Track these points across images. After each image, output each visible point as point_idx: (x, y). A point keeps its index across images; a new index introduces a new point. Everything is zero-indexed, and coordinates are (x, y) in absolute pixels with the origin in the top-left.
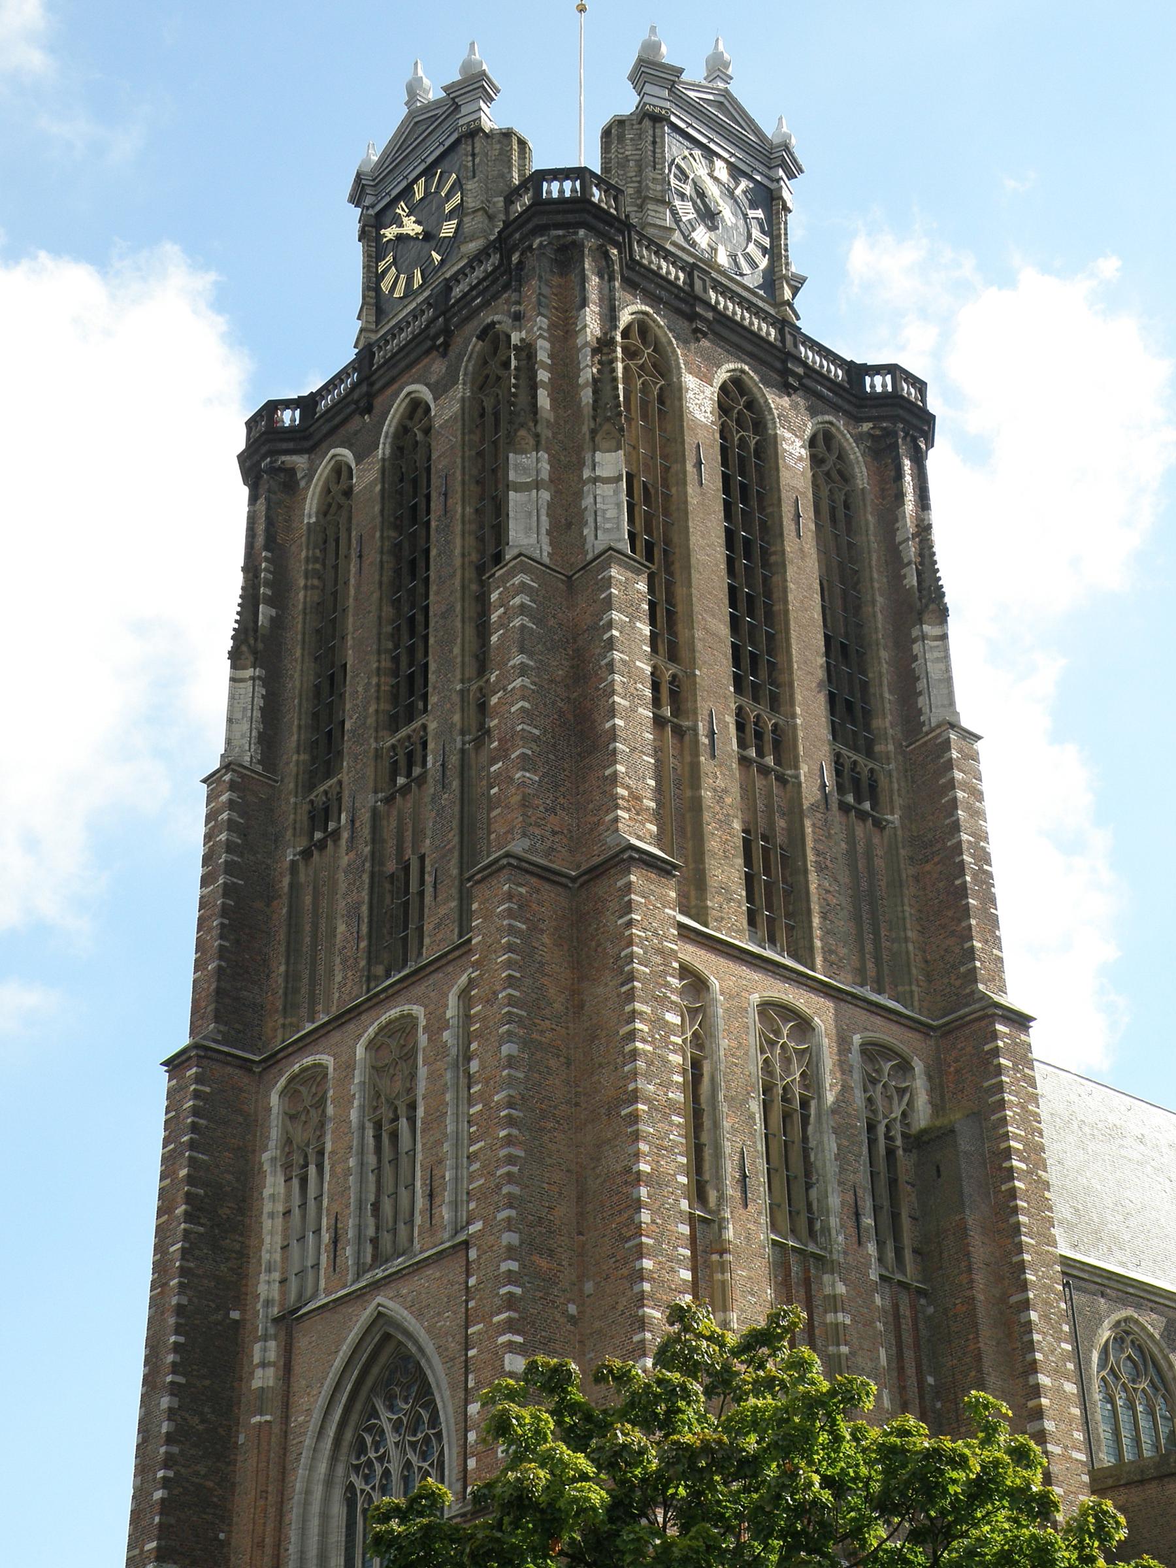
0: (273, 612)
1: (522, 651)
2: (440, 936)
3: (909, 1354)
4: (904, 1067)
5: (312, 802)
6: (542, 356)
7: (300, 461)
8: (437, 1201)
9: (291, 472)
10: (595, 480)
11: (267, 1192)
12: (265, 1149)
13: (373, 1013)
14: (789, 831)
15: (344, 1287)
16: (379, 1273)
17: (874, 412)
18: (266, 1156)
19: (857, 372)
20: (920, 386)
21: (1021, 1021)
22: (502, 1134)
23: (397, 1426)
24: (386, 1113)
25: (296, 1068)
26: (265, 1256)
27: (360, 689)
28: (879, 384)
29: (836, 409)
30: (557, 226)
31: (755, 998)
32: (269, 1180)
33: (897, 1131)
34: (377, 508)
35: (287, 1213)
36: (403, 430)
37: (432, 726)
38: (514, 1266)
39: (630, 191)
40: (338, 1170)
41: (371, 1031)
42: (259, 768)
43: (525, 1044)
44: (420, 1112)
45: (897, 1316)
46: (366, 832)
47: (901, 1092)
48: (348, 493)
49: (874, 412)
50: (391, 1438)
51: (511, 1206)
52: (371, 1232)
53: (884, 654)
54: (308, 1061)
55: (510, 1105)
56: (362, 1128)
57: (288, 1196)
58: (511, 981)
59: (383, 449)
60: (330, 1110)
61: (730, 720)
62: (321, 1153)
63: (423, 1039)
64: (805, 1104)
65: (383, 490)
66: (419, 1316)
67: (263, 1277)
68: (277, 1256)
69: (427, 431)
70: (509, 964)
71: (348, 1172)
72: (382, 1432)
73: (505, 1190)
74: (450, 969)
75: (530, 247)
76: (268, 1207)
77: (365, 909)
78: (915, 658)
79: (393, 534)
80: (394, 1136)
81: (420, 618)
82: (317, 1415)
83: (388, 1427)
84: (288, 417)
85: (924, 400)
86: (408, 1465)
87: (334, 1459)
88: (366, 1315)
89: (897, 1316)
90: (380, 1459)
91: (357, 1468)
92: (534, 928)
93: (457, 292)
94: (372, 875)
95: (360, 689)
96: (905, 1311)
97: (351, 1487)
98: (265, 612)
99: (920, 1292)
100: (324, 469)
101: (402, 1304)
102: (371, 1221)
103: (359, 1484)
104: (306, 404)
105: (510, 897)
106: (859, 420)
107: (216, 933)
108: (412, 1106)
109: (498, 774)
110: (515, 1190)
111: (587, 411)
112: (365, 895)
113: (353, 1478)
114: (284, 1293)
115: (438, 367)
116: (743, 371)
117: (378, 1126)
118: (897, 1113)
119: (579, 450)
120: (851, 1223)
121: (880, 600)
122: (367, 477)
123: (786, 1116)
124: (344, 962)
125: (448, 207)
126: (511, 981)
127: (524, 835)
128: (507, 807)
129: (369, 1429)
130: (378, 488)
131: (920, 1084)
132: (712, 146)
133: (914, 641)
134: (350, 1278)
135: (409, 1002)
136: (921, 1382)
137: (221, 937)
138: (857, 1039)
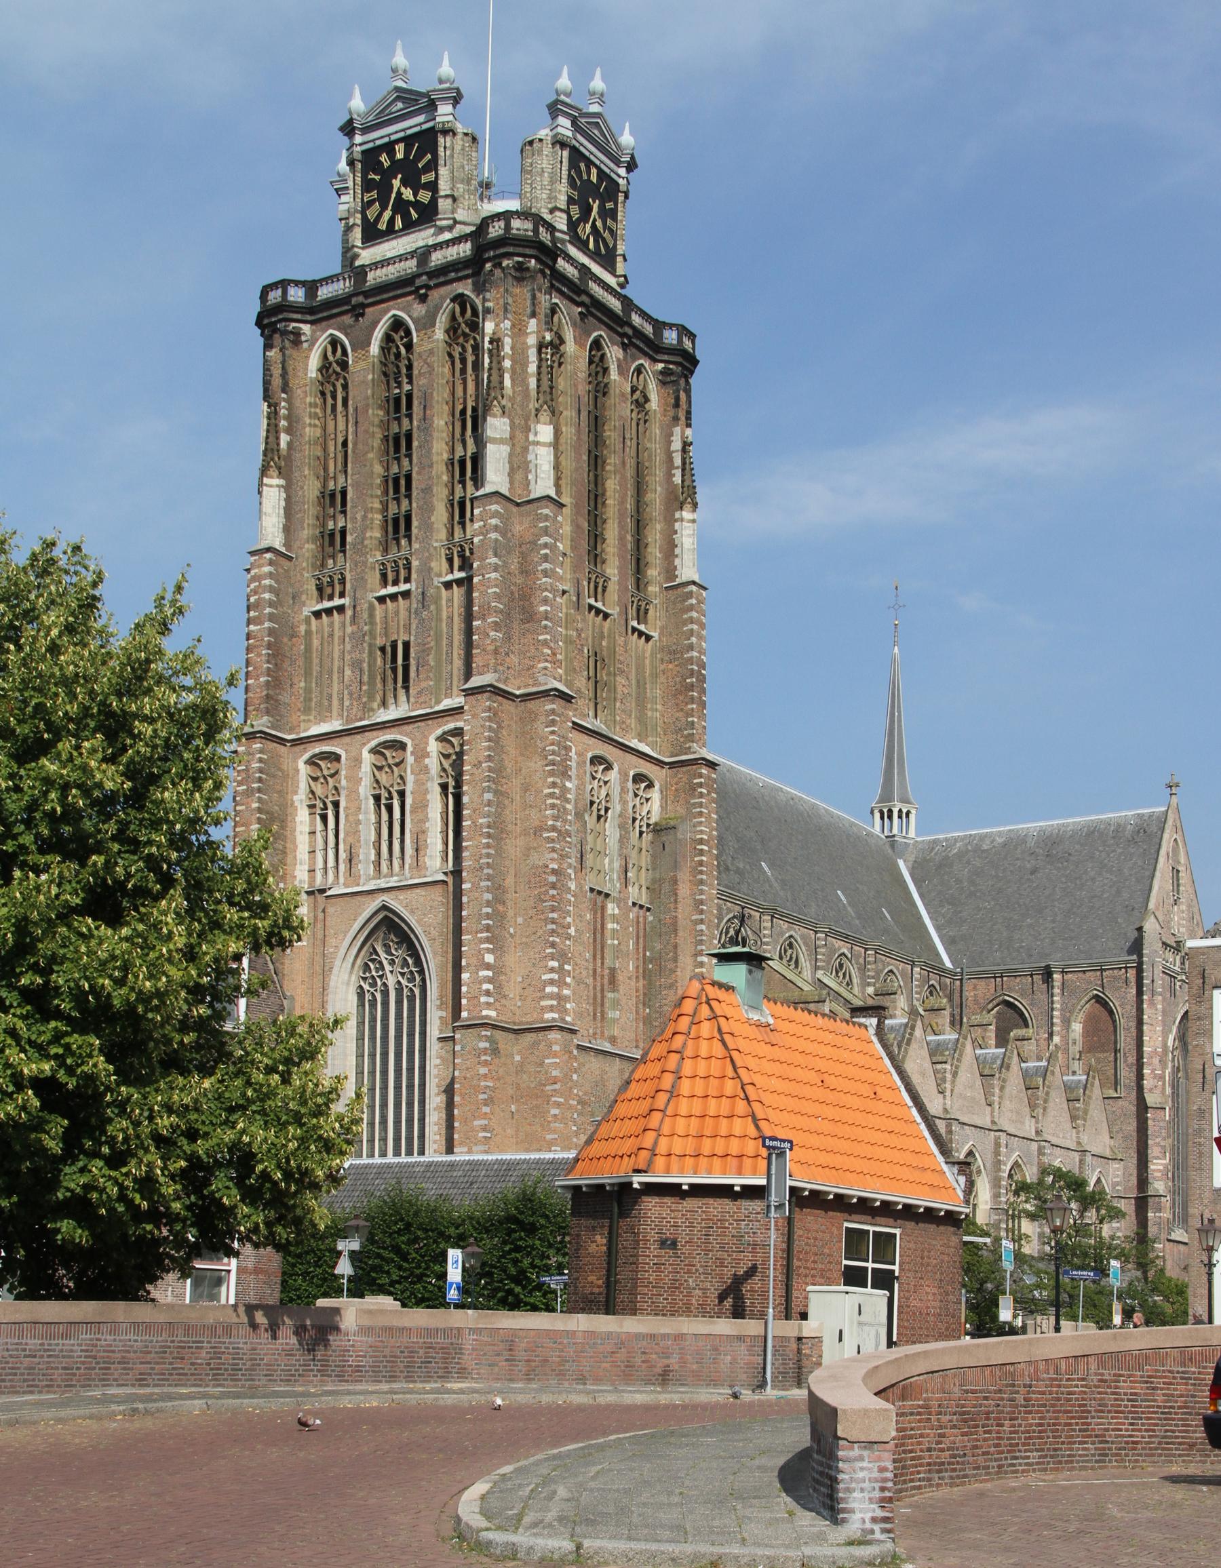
0: (288, 438)
1: (496, 555)
2: (421, 700)
3: (641, 940)
4: (650, 786)
6: (507, 349)
7: (306, 328)
8: (421, 853)
9: (297, 334)
10: (538, 443)
11: (298, 819)
12: (296, 793)
13: (375, 733)
14: (608, 647)
15: (358, 885)
16: (383, 883)
17: (666, 357)
18: (295, 798)
19: (659, 326)
20: (692, 336)
21: (712, 765)
22: (484, 841)
23: (392, 962)
24: (384, 794)
26: (299, 856)
27: (359, 516)
28: (670, 337)
29: (646, 354)
30: (519, 255)
31: (590, 755)
32: (299, 812)
33: (644, 823)
34: (369, 392)
35: (313, 833)
36: (388, 338)
37: (415, 563)
38: (489, 910)
39: (544, 196)
40: (351, 818)
41: (373, 743)
42: (283, 550)
43: (496, 792)
44: (409, 801)
45: (638, 922)
46: (365, 616)
47: (647, 800)
48: (344, 365)
49: (666, 357)
50: (388, 967)
51: (488, 880)
52: (373, 857)
53: (658, 527)
54: (326, 748)
55: (489, 827)
57: (312, 823)
58: (489, 758)
59: (375, 349)
60: (344, 782)
61: (585, 583)
62: (336, 805)
63: (410, 759)
64: (607, 809)
65: (373, 380)
66: (412, 912)
67: (298, 867)
68: (307, 856)
69: (409, 347)
70: (489, 748)
72: (381, 963)
73: (486, 871)
74: (430, 722)
75: (500, 264)
76: (298, 829)
77: (365, 665)
78: (676, 532)
79: (381, 413)
80: (390, 808)
81: (403, 482)
82: (342, 951)
83: (385, 963)
84: (297, 295)
85: (694, 348)
86: (399, 982)
87: (351, 973)
88: (375, 904)
89: (638, 922)
90: (381, 977)
91: (365, 979)
92: (500, 727)
93: (437, 258)
94: (370, 645)
95: (359, 516)
96: (641, 919)
97: (361, 987)
98: (284, 439)
99: (648, 909)
100: (323, 340)
101: (401, 904)
102: (373, 852)
103: (366, 987)
104: (311, 287)
105: (490, 709)
106: (655, 361)
107: (264, 658)
108: (402, 794)
109: (478, 628)
110: (490, 871)
111: (533, 393)
112: (365, 655)
113: (362, 983)
114: (312, 879)
115: (419, 309)
116: (601, 336)
117: (377, 798)
118: (644, 813)
119: (527, 419)
120: (623, 877)
121: (659, 489)
123: (599, 817)
124: (351, 694)
125: (424, 179)
126: (489, 758)
127: (496, 671)
128: (484, 650)
129: (373, 960)
130: (370, 377)
131: (655, 795)
132: (592, 158)
133: (676, 521)
135: (400, 733)
136: (645, 955)
137: (268, 662)
138: (632, 773)
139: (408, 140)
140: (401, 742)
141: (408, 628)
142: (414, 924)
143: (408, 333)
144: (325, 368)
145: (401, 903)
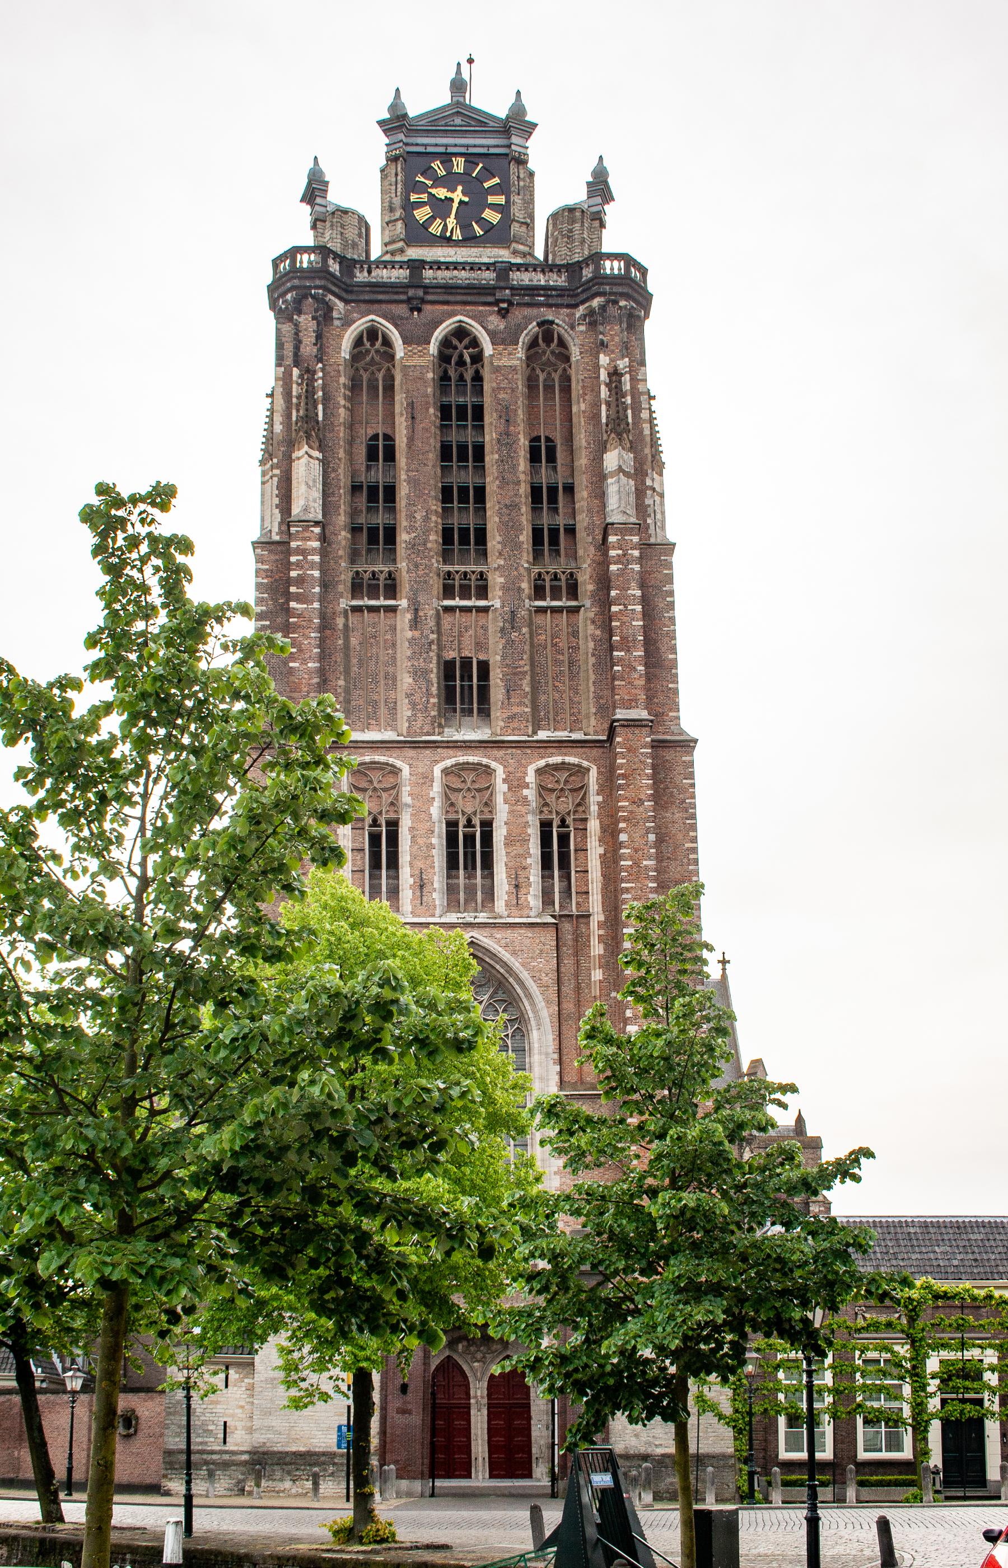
5: (357, 573)
13: (451, 752)
25: (367, 759)
36: (446, 343)
41: (449, 763)
56: (440, 822)
59: (433, 348)
71: (431, 846)
115: (495, 322)
122: (415, 360)
124: (413, 705)
134: (438, 912)
139: (471, 159)
140: (487, 767)
141: (480, 645)
142: (515, 964)
143: (475, 343)
144: (357, 356)
145: (498, 942)
